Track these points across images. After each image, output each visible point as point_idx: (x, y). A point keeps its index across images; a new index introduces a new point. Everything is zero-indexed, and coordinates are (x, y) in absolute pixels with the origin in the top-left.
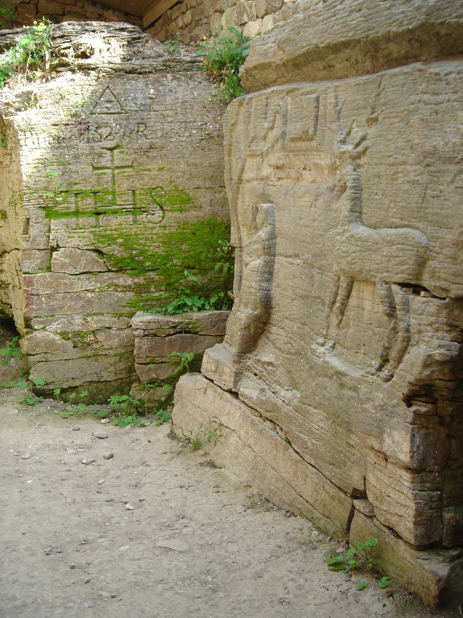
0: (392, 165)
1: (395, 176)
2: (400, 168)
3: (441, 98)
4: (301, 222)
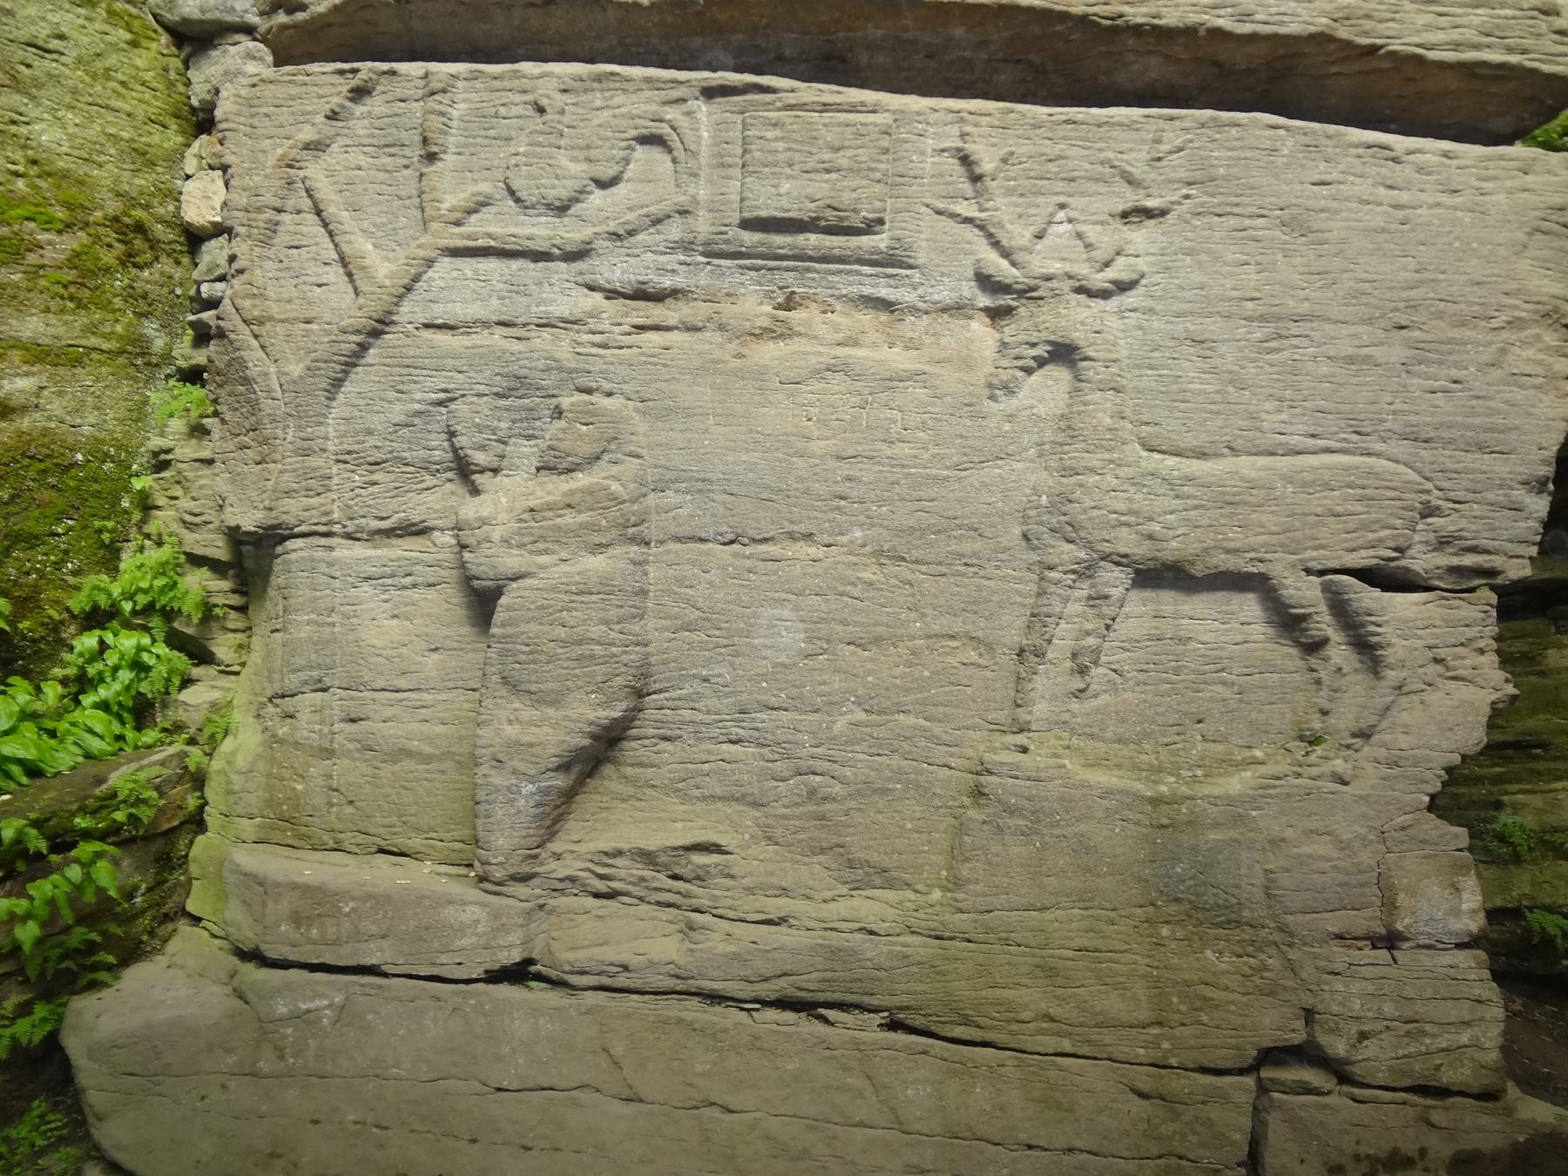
0: (1262, 318)
1: (1273, 344)
2: (1295, 329)
3: (1404, 197)
4: (817, 447)
